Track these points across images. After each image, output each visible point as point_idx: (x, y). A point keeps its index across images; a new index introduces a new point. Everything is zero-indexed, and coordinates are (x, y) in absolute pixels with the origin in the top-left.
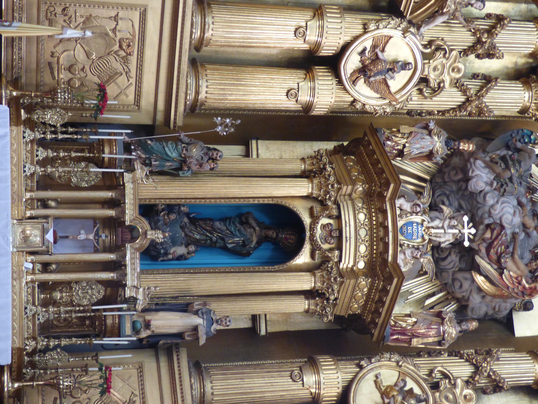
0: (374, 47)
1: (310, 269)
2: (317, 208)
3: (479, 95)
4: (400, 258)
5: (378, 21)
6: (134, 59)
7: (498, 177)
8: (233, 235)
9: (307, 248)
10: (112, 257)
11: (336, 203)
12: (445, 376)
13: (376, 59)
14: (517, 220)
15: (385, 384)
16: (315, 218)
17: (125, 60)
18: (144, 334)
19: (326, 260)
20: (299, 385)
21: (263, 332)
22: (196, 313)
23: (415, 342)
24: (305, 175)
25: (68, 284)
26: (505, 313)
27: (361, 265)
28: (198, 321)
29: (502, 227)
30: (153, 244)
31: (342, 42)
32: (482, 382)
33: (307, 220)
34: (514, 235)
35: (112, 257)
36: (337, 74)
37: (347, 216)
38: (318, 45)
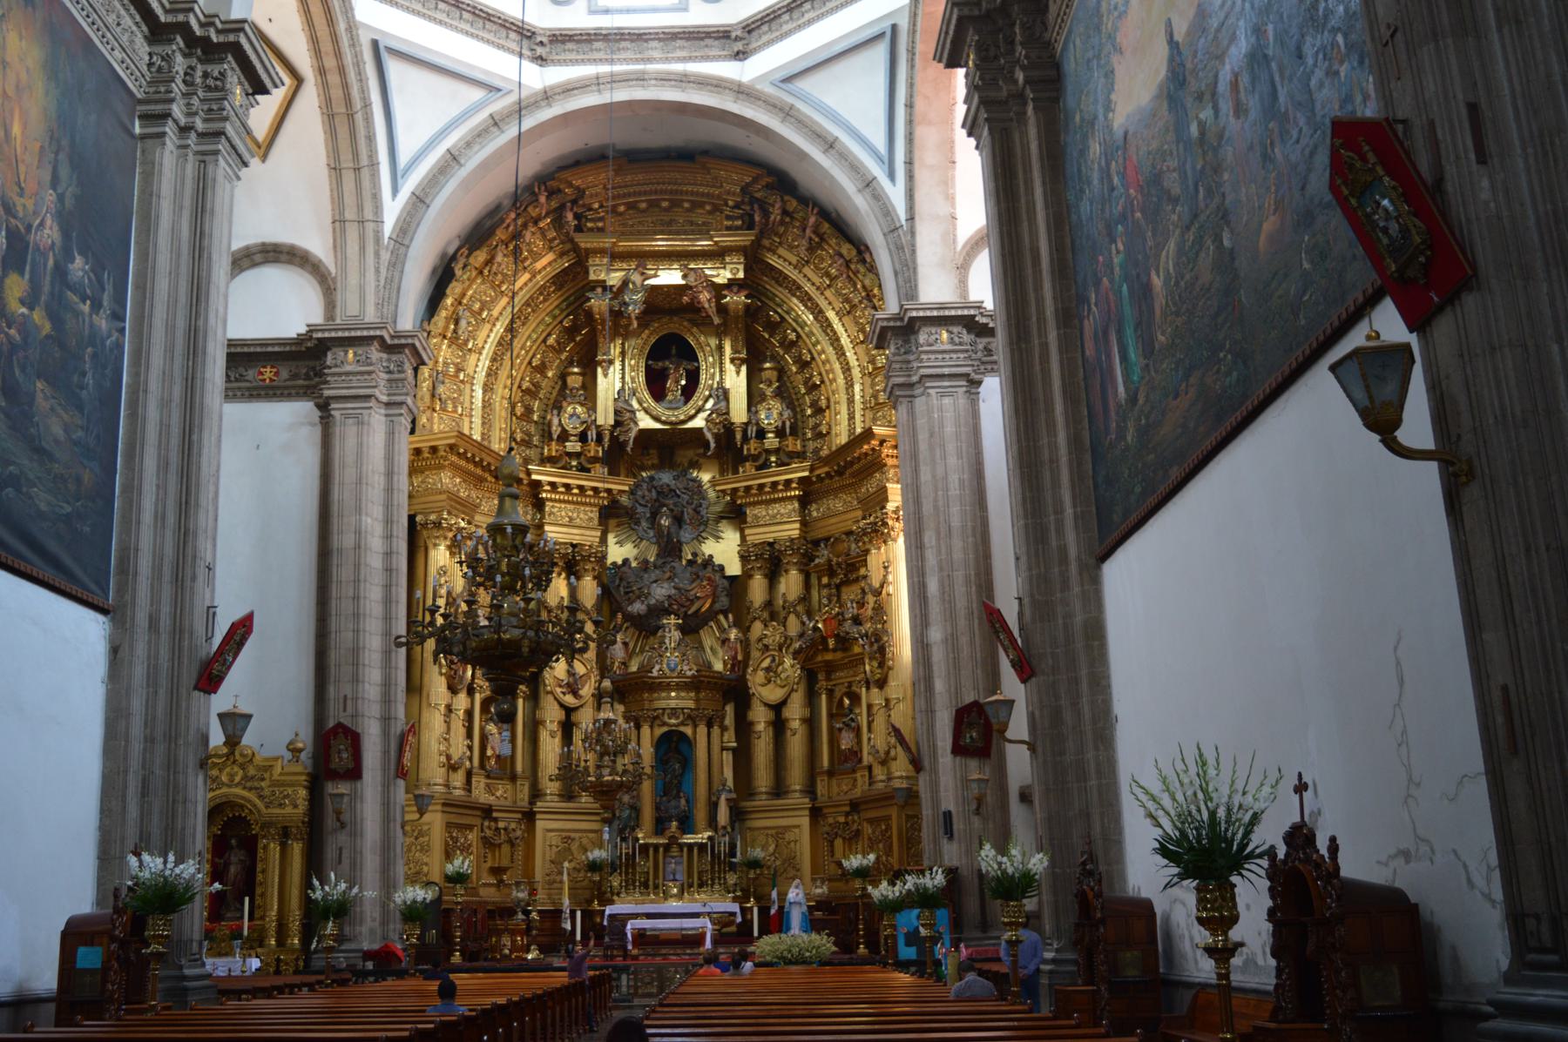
0: (560, 686)
1: (695, 726)
2: (658, 722)
3: (587, 613)
4: (689, 673)
5: (545, 685)
6: (573, 835)
7: (639, 597)
8: (674, 770)
9: (682, 729)
10: (685, 849)
11: (655, 710)
12: (760, 640)
13: (568, 685)
14: (666, 585)
15: (764, 681)
16: (664, 724)
17: (573, 839)
18: (729, 829)
19: (689, 717)
20: (763, 735)
21: (735, 745)
22: (718, 798)
23: (740, 657)
24: (638, 727)
25: (700, 873)
26: (726, 583)
27: (693, 694)
28: (723, 798)
29: (670, 596)
30: (678, 828)
31: (556, 706)
32: (766, 615)
33: (665, 729)
34: (675, 588)
35: (685, 849)
36: (576, 709)
37: (662, 704)
38: (559, 722)
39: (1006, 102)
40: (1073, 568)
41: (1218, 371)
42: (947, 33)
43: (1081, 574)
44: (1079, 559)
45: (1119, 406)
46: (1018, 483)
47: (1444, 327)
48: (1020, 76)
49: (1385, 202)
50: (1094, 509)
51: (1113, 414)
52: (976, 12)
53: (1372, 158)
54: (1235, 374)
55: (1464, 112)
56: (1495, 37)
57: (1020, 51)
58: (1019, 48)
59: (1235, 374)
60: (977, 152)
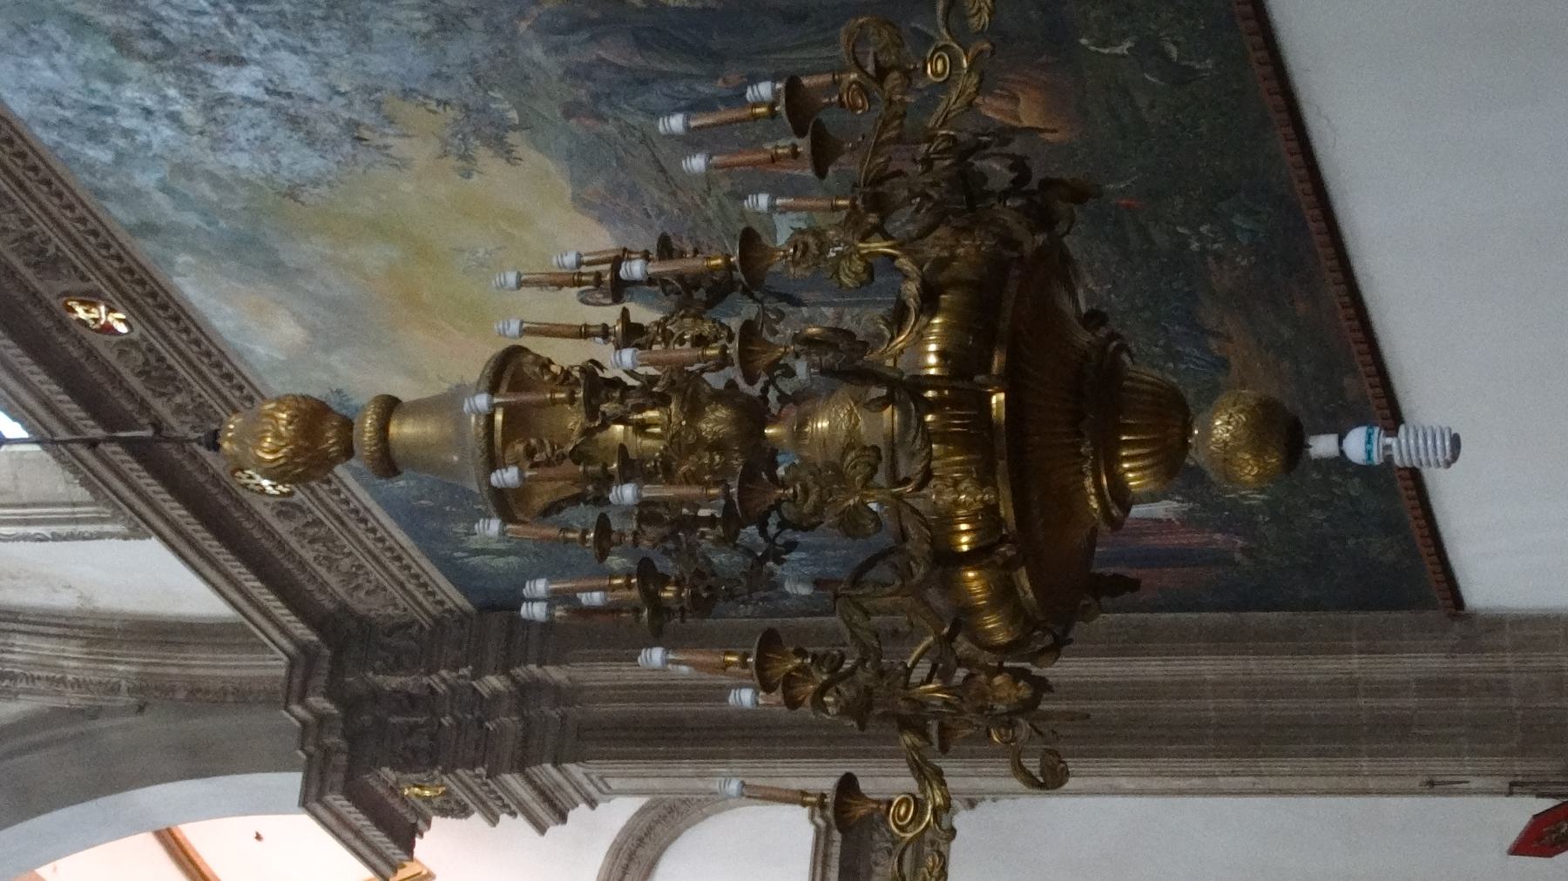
39: (527, 721)
40: (1467, 663)
41: (1219, 257)
42: (358, 834)
43: (1482, 650)
44: (1452, 651)
45: (1187, 521)
46: (1286, 766)
48: (494, 682)
50: (1357, 617)
51: (1197, 539)
52: (342, 760)
54: (1238, 220)
57: (439, 682)
58: (434, 680)
59: (1238, 220)
60: (601, 806)
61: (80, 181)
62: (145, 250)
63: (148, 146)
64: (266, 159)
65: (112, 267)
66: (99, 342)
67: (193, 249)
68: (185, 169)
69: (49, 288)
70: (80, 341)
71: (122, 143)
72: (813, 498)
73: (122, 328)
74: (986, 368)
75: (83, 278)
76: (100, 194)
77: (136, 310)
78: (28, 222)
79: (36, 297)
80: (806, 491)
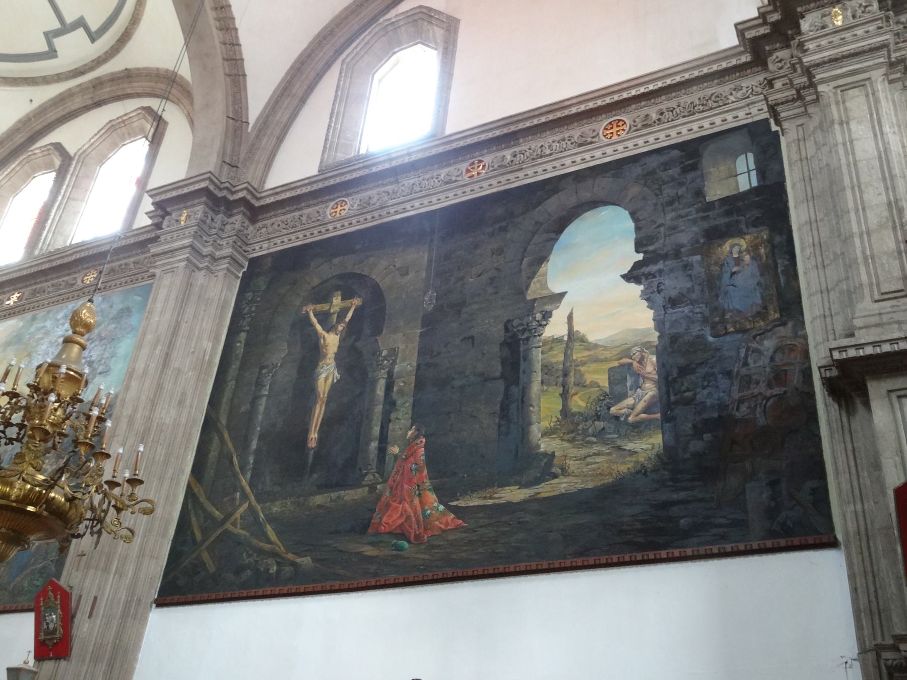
47: (49, 665)
49: (54, 616)
53: (58, 602)
55: (93, 598)
56: (112, 576)
61: (55, 308)
62: (28, 316)
63: (58, 327)
64: (41, 353)
65: (27, 307)
66: (6, 296)
67: (23, 327)
68: (47, 333)
69: (27, 291)
70: (8, 292)
71: (62, 321)
72: (33, 448)
73: (7, 303)
74: (46, 510)
75: (27, 299)
76: (49, 312)
77: (12, 308)
78: (49, 293)
79: (27, 286)
80: (36, 447)
